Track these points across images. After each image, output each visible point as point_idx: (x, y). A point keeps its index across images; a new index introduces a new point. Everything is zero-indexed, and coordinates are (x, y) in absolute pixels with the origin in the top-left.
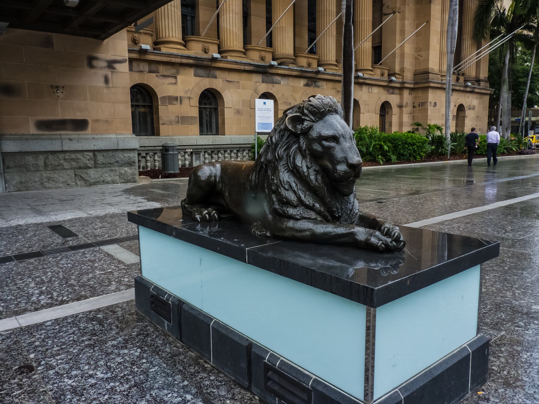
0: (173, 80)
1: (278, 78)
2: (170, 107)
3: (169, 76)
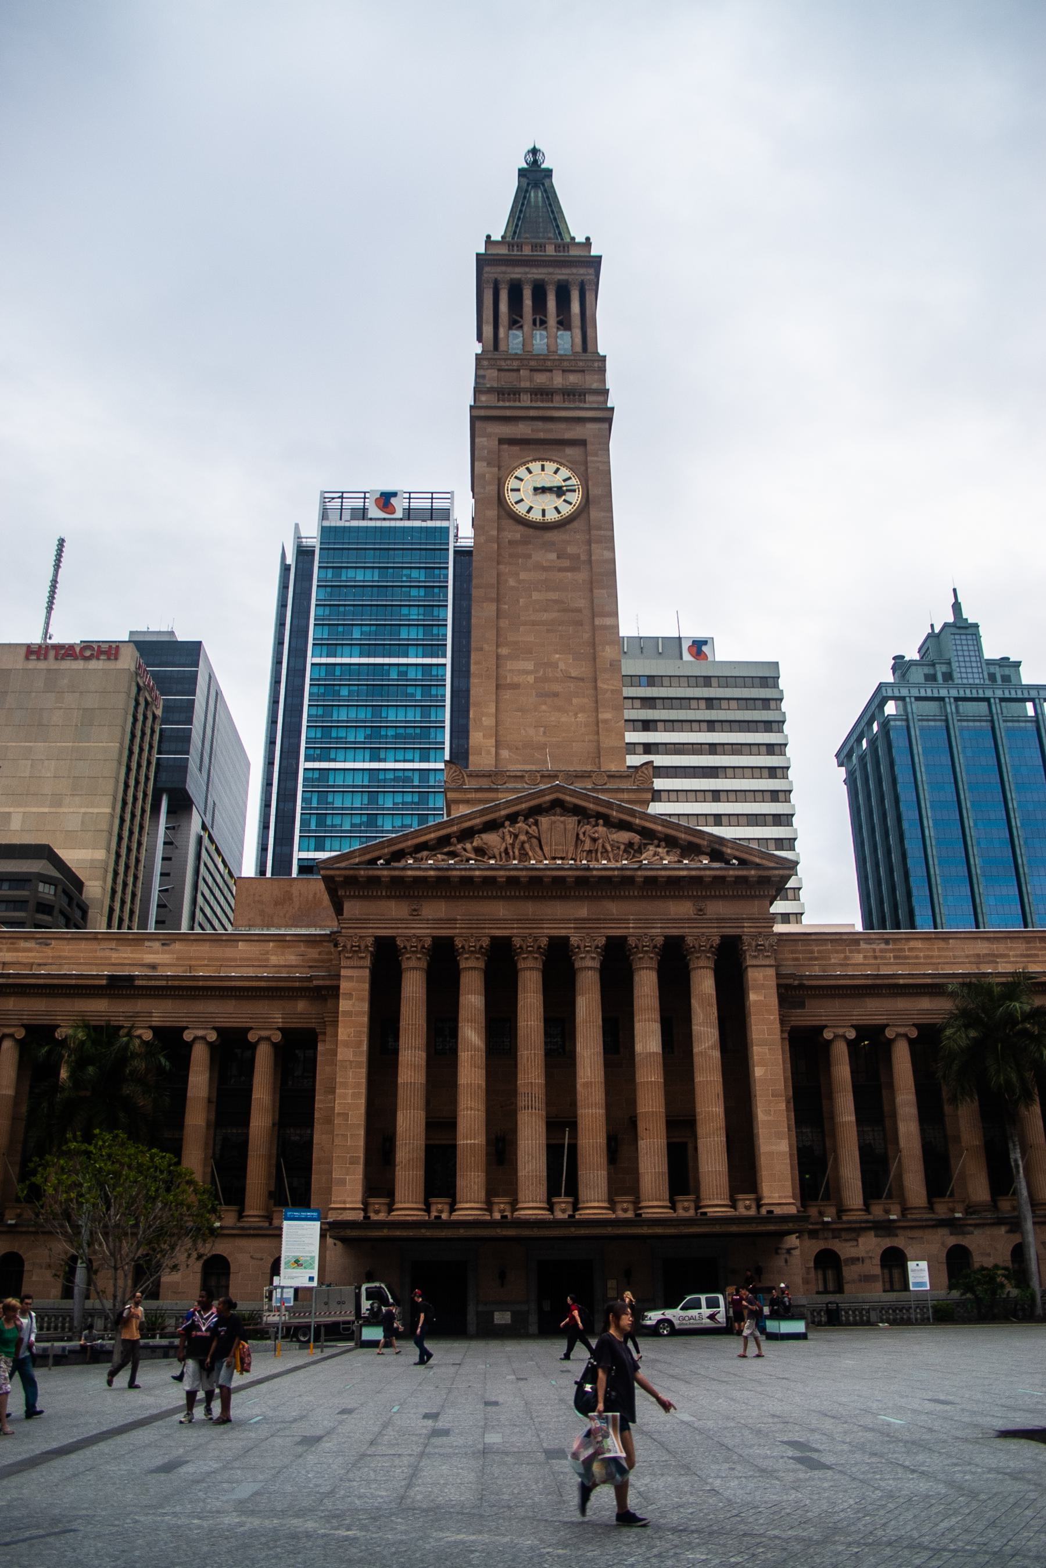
0: (855, 1243)
1: (971, 1229)
2: (854, 1268)
3: (851, 1240)
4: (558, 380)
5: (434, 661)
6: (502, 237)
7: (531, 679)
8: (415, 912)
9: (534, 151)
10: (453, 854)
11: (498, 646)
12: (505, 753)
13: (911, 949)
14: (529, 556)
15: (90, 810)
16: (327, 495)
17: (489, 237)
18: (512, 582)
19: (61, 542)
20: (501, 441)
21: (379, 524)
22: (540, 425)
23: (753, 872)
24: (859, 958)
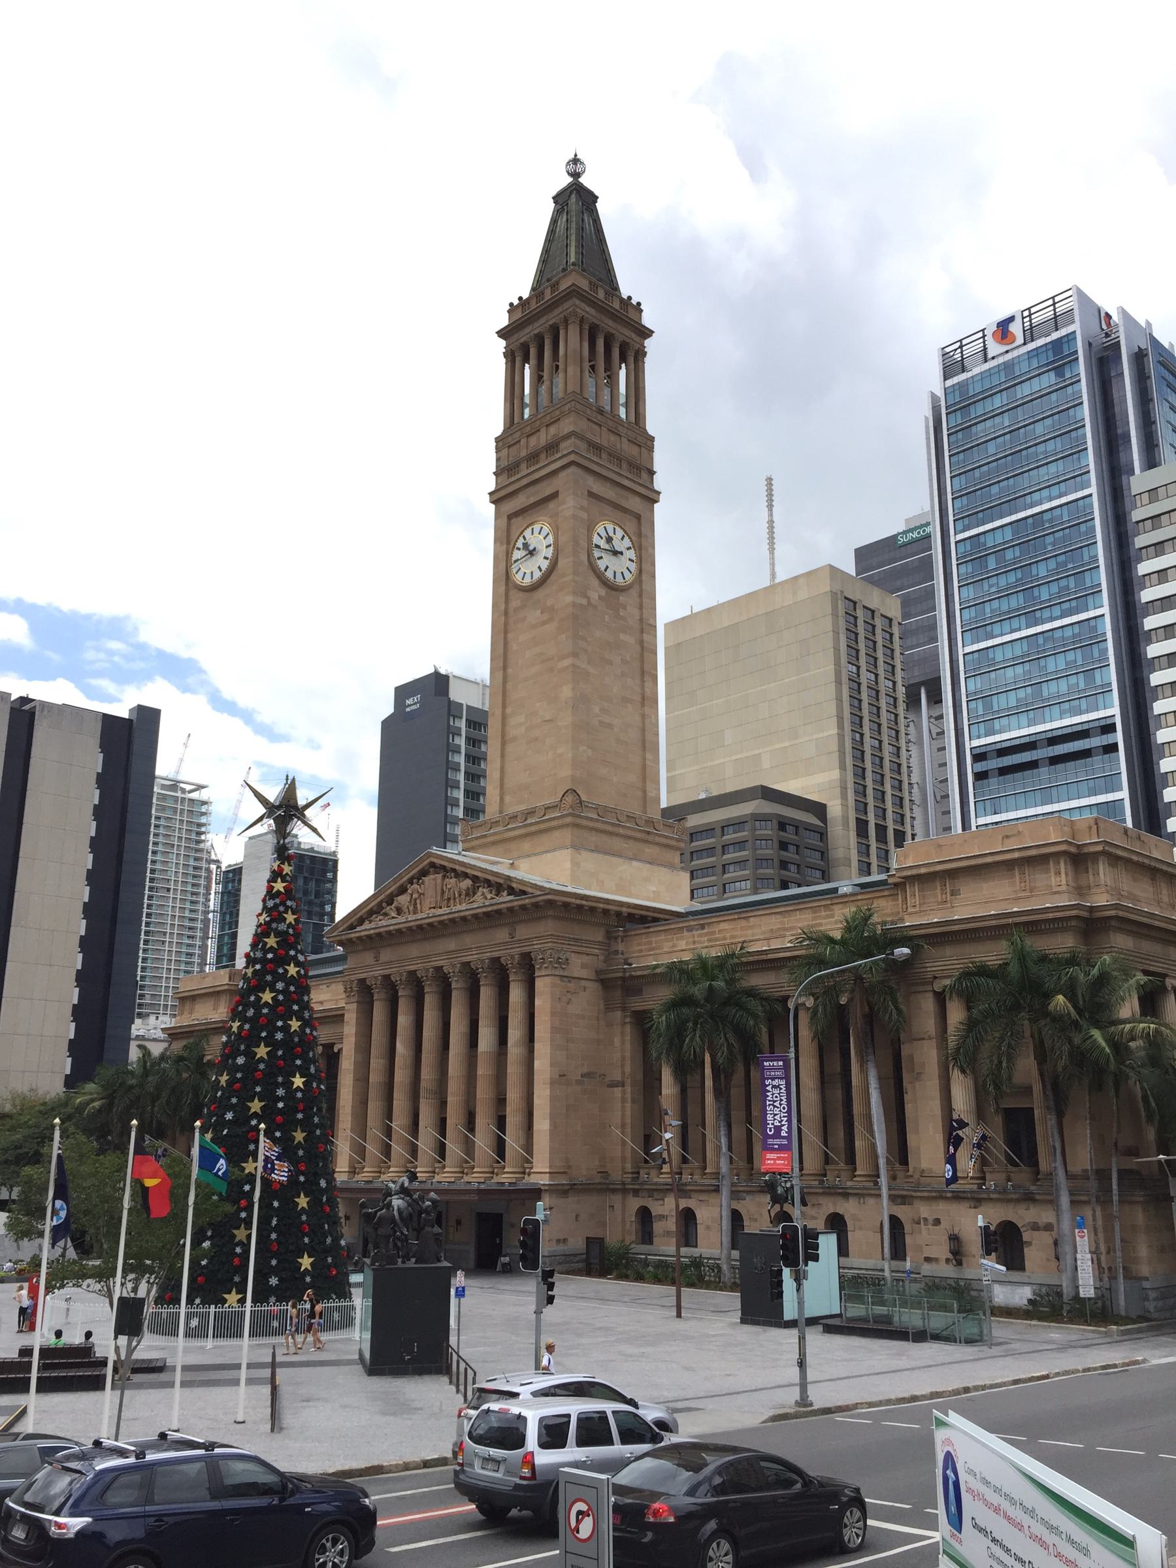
4: (542, 438)
6: (520, 298)
7: (523, 729)
8: (377, 959)
9: (576, 161)
10: (386, 914)
11: (504, 706)
12: (507, 799)
13: (720, 931)
14: (525, 619)
15: (821, 735)
16: (948, 350)
17: (511, 304)
18: (515, 647)
19: (769, 480)
20: (510, 517)
21: (1001, 360)
22: (531, 489)
23: (527, 901)
24: (682, 944)
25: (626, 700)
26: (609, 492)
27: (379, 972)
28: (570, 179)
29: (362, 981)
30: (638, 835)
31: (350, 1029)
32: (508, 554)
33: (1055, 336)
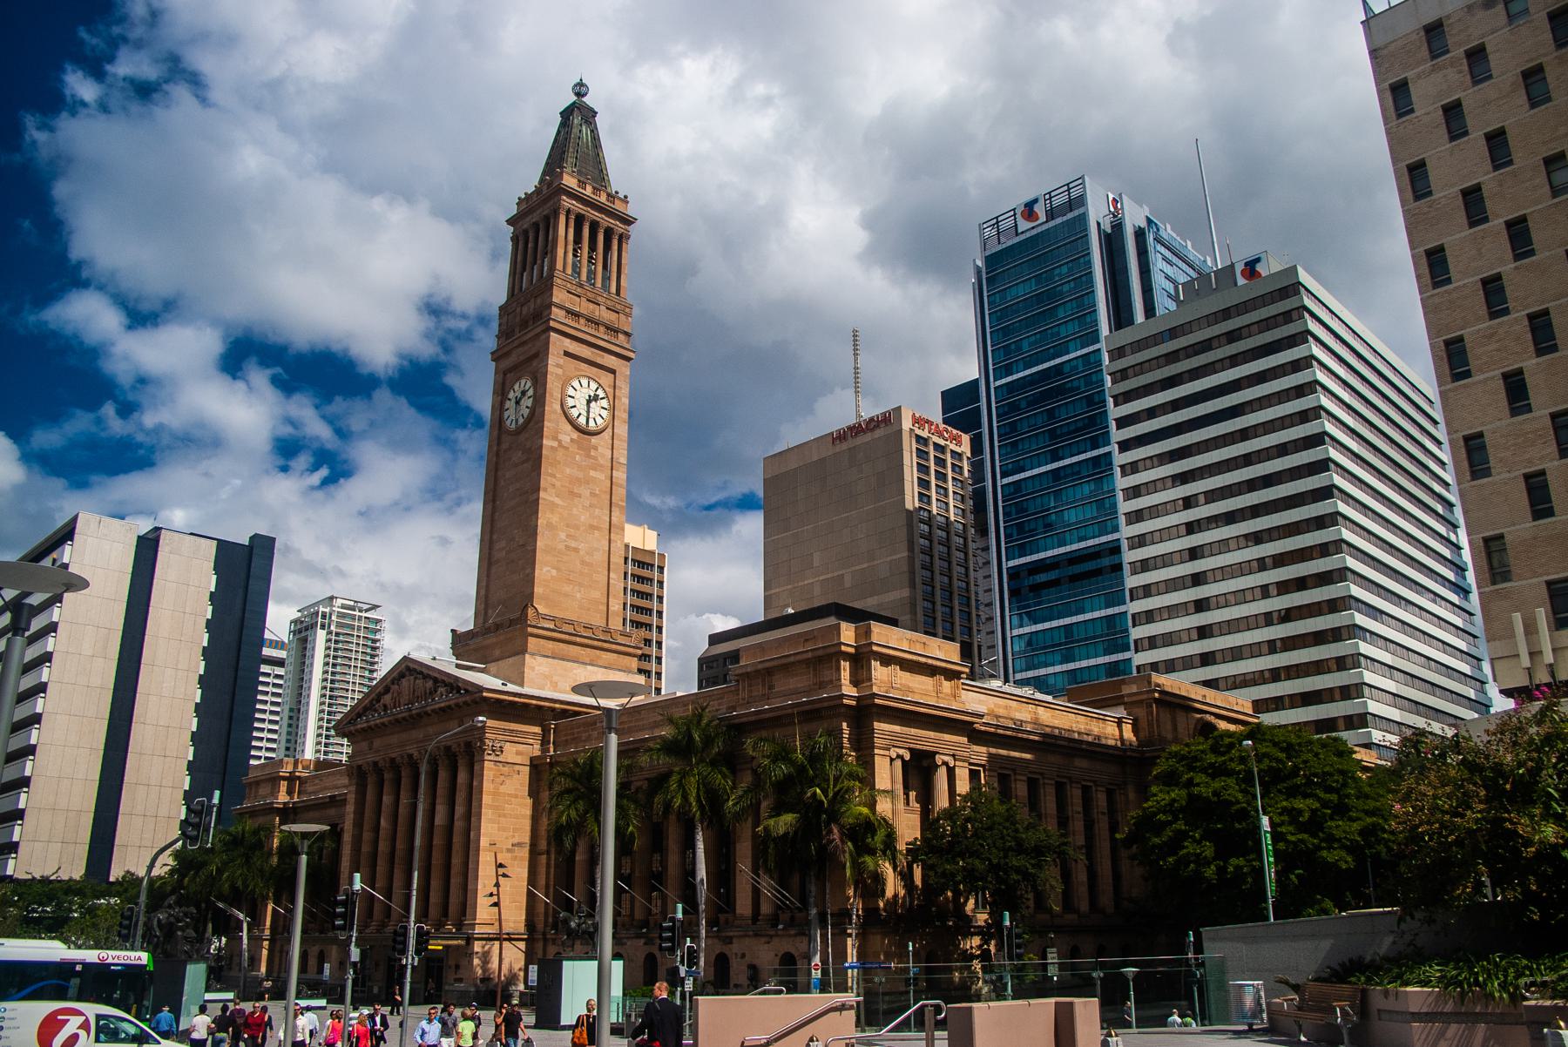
5: (1091, 348)
9: (581, 84)
21: (1028, 235)
25: (592, 527)
26: (585, 352)
27: (371, 758)
28: (575, 98)
29: (359, 767)
30: (596, 643)
31: (350, 808)
32: (502, 403)
33: (1070, 216)
